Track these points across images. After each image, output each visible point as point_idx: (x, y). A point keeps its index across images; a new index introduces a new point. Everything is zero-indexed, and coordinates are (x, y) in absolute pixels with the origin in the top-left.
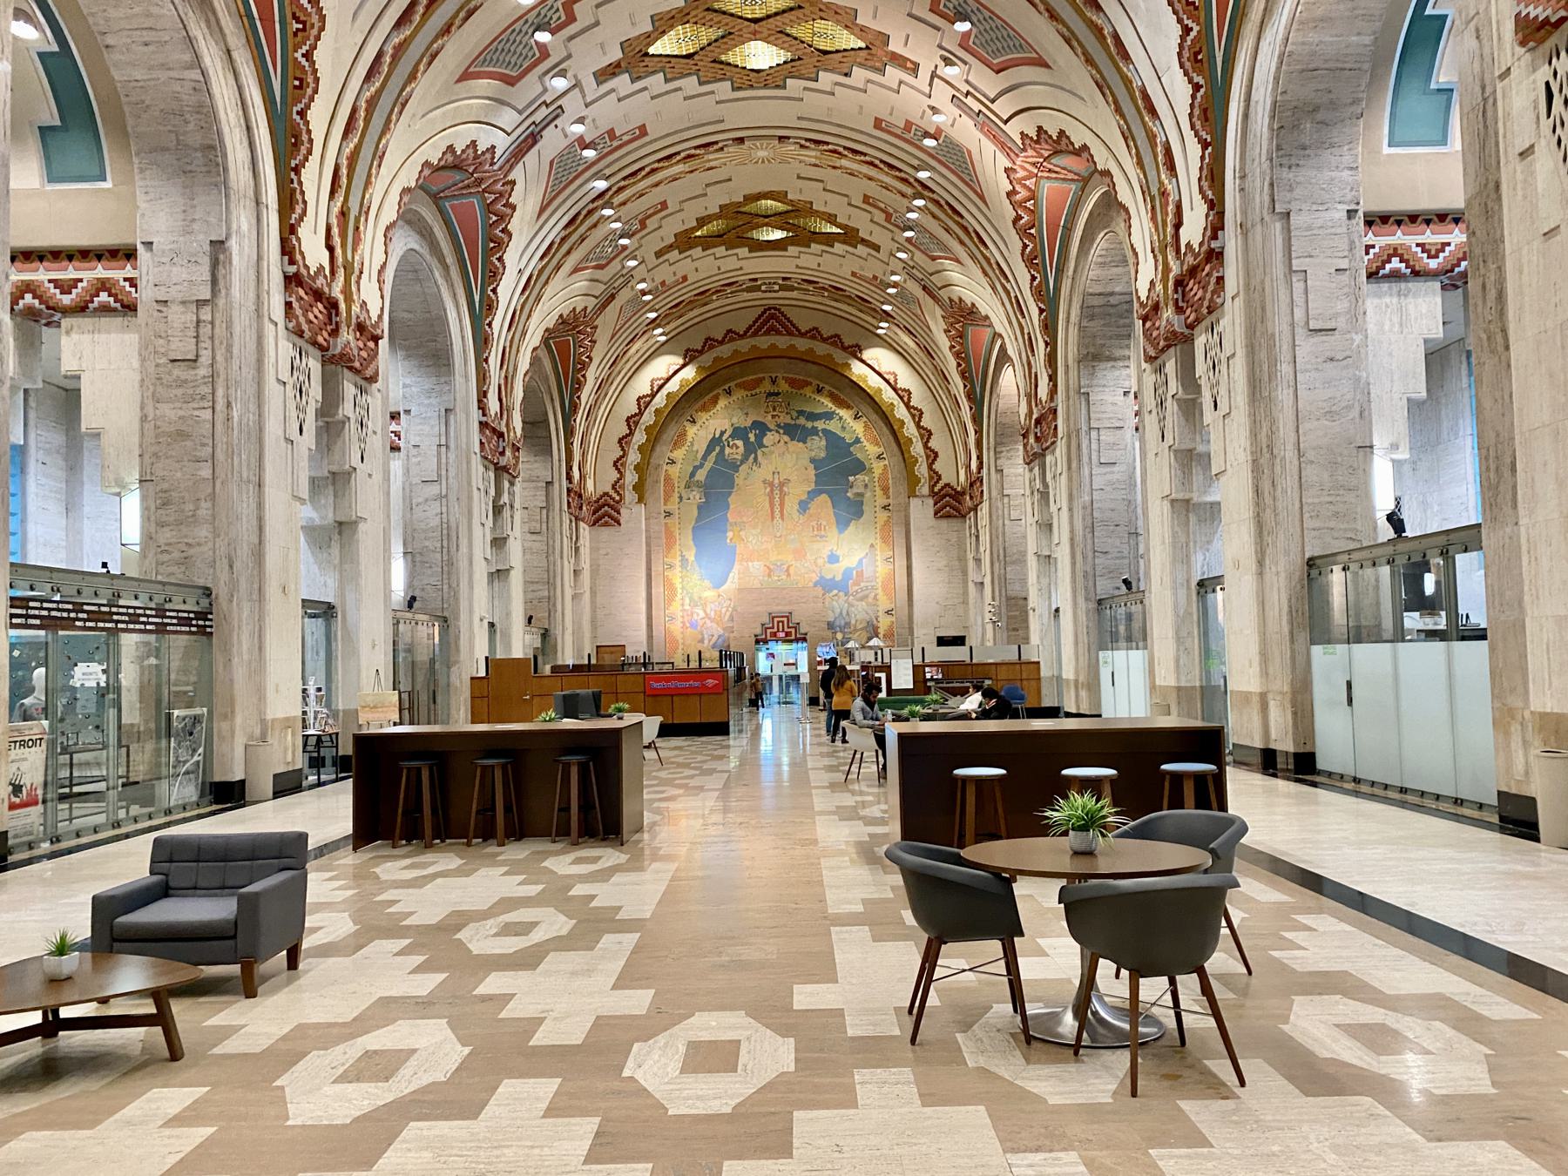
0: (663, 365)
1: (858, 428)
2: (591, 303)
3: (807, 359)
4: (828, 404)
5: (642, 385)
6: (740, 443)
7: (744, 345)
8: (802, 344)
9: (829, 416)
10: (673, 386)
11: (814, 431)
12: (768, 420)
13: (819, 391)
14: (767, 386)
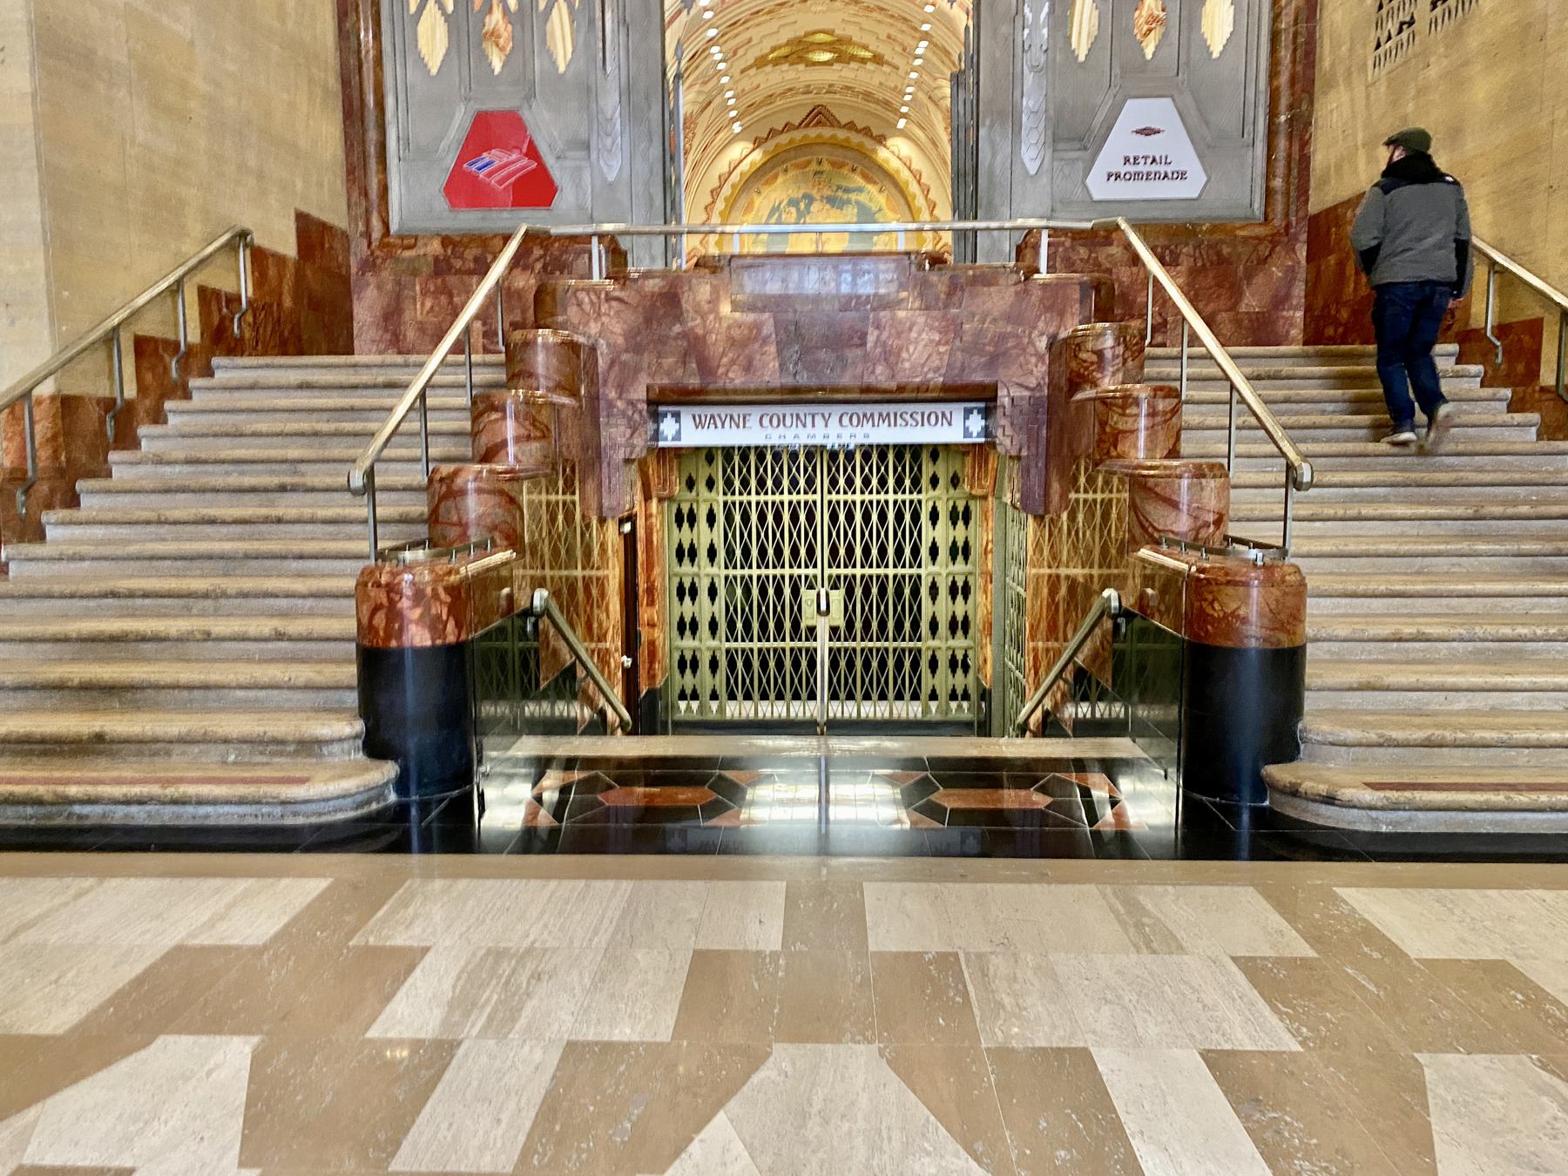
0: (738, 150)
1: (882, 199)
2: (696, 108)
3: (845, 146)
4: (858, 180)
5: (722, 166)
6: (793, 210)
7: (798, 135)
8: (841, 134)
9: (860, 190)
10: (745, 166)
11: (849, 202)
12: (814, 192)
13: (854, 170)
14: (814, 167)
